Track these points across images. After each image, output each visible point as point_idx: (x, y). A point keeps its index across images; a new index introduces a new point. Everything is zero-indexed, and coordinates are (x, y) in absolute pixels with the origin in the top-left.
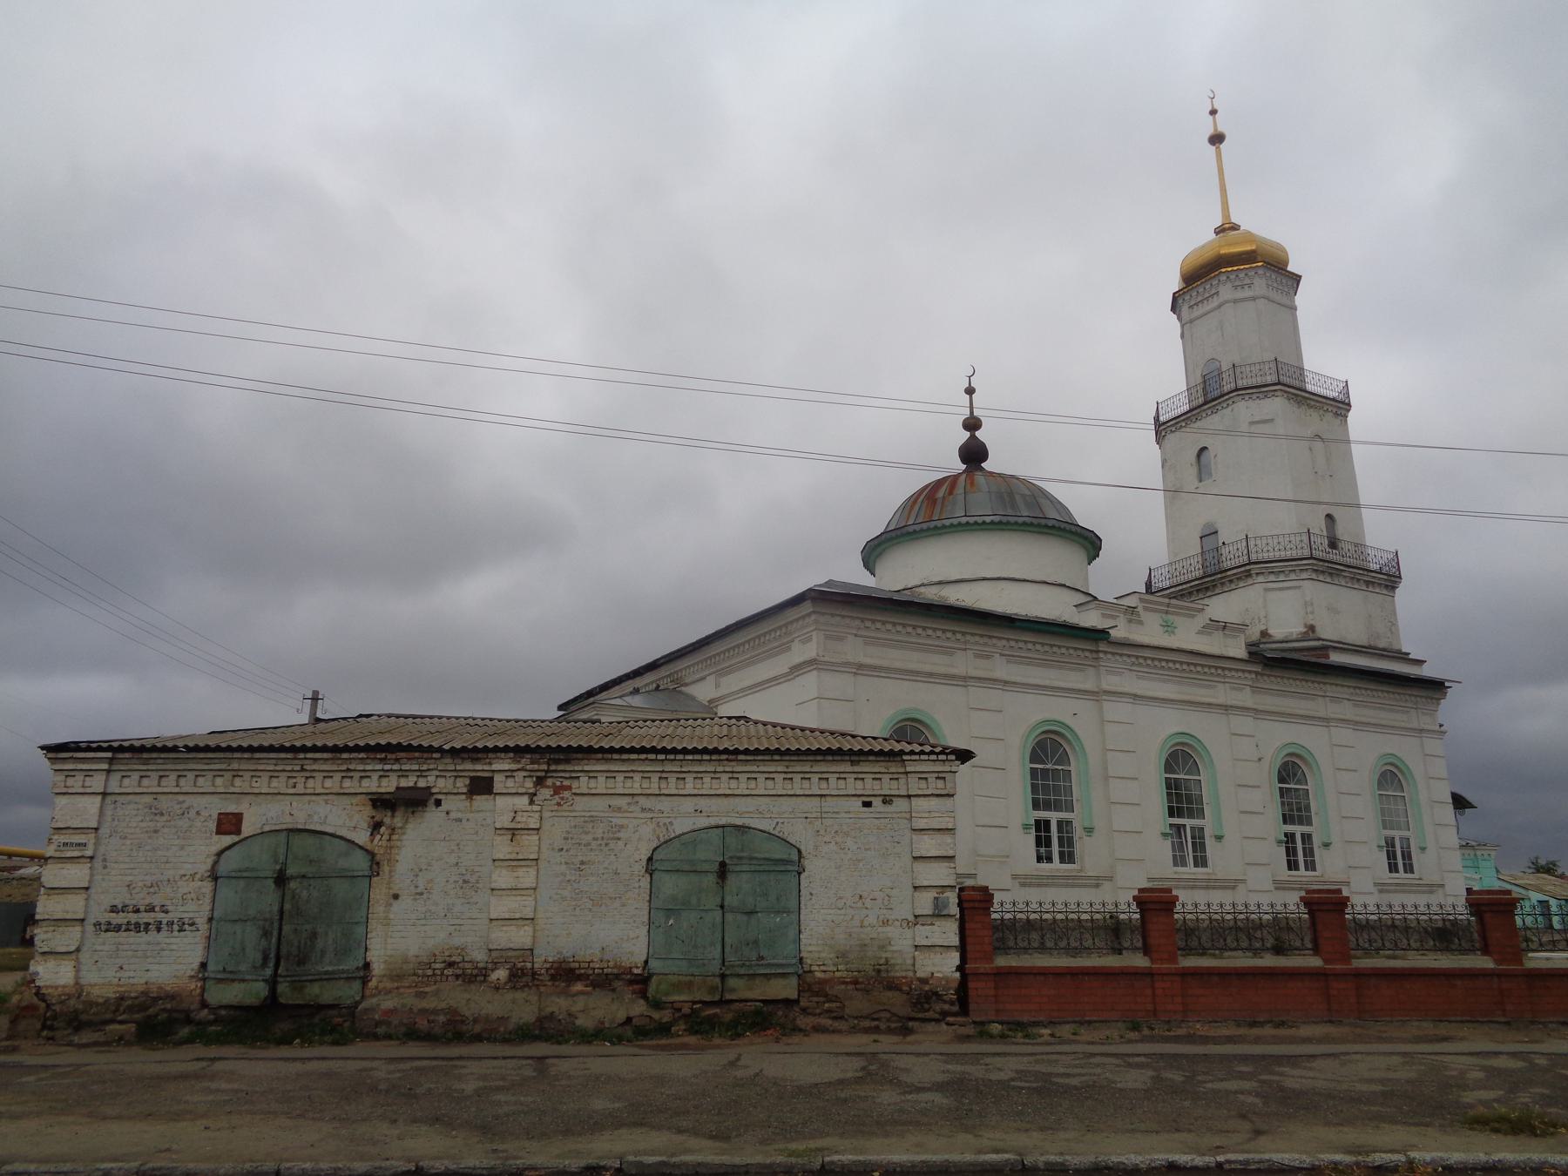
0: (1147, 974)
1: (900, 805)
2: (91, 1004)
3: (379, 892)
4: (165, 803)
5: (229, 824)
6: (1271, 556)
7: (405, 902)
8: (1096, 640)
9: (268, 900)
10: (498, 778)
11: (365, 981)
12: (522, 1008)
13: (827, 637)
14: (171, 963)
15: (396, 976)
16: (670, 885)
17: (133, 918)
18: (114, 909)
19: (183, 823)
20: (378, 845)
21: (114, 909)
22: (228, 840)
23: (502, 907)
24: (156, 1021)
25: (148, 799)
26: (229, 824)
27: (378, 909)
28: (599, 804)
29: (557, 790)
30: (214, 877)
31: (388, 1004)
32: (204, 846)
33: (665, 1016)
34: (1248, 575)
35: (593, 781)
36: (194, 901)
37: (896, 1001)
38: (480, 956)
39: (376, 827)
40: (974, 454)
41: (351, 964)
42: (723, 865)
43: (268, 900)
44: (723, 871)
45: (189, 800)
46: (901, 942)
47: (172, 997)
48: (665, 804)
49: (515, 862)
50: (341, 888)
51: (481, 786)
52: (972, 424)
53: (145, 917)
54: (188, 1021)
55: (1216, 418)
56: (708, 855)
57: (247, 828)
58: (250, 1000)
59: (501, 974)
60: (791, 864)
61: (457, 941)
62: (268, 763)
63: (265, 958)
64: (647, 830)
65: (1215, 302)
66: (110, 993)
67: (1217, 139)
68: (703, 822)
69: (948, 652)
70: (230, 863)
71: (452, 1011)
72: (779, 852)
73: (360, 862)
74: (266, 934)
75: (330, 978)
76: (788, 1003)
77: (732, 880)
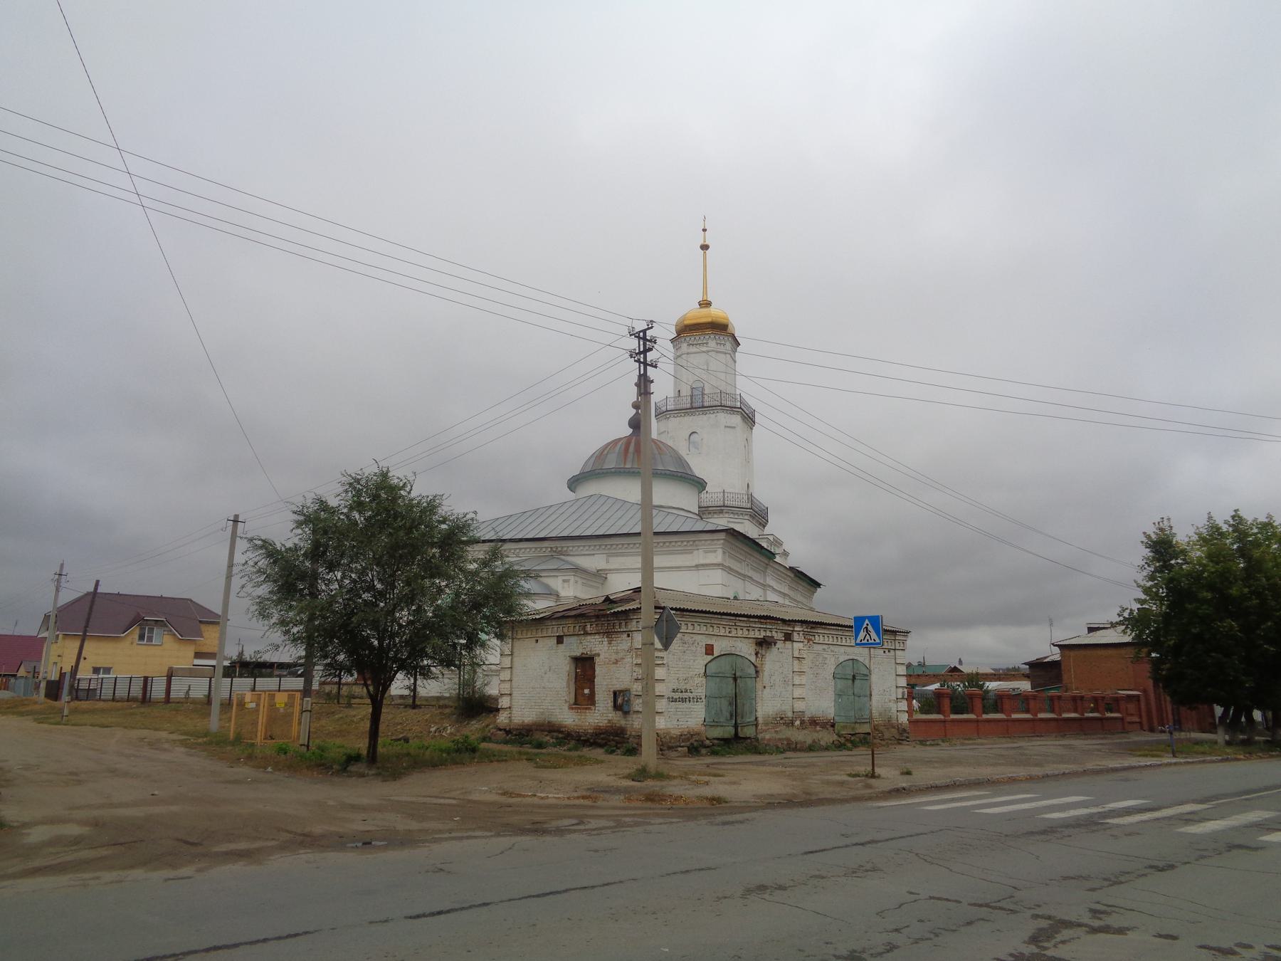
0: (945, 721)
2: (671, 738)
3: (759, 686)
5: (709, 650)
6: (734, 504)
7: (767, 690)
9: (729, 688)
11: (756, 726)
14: (692, 718)
15: (766, 724)
17: (681, 695)
18: (674, 691)
21: (674, 691)
22: (710, 658)
23: (798, 692)
24: (694, 746)
26: (709, 650)
28: (820, 647)
29: (809, 640)
31: (767, 737)
33: (842, 740)
34: (721, 512)
35: (821, 637)
36: (700, 687)
38: (790, 714)
39: (757, 654)
43: (729, 688)
44: (854, 677)
45: (696, 637)
46: (894, 707)
48: (836, 649)
50: (749, 682)
51: (788, 637)
53: (685, 695)
55: (705, 417)
56: (849, 672)
58: (726, 736)
59: (798, 723)
60: (866, 677)
66: (676, 732)
67: (705, 247)
68: (847, 658)
69: (740, 561)
70: (713, 668)
71: (788, 739)
73: (752, 671)
74: (730, 704)
77: (857, 682)
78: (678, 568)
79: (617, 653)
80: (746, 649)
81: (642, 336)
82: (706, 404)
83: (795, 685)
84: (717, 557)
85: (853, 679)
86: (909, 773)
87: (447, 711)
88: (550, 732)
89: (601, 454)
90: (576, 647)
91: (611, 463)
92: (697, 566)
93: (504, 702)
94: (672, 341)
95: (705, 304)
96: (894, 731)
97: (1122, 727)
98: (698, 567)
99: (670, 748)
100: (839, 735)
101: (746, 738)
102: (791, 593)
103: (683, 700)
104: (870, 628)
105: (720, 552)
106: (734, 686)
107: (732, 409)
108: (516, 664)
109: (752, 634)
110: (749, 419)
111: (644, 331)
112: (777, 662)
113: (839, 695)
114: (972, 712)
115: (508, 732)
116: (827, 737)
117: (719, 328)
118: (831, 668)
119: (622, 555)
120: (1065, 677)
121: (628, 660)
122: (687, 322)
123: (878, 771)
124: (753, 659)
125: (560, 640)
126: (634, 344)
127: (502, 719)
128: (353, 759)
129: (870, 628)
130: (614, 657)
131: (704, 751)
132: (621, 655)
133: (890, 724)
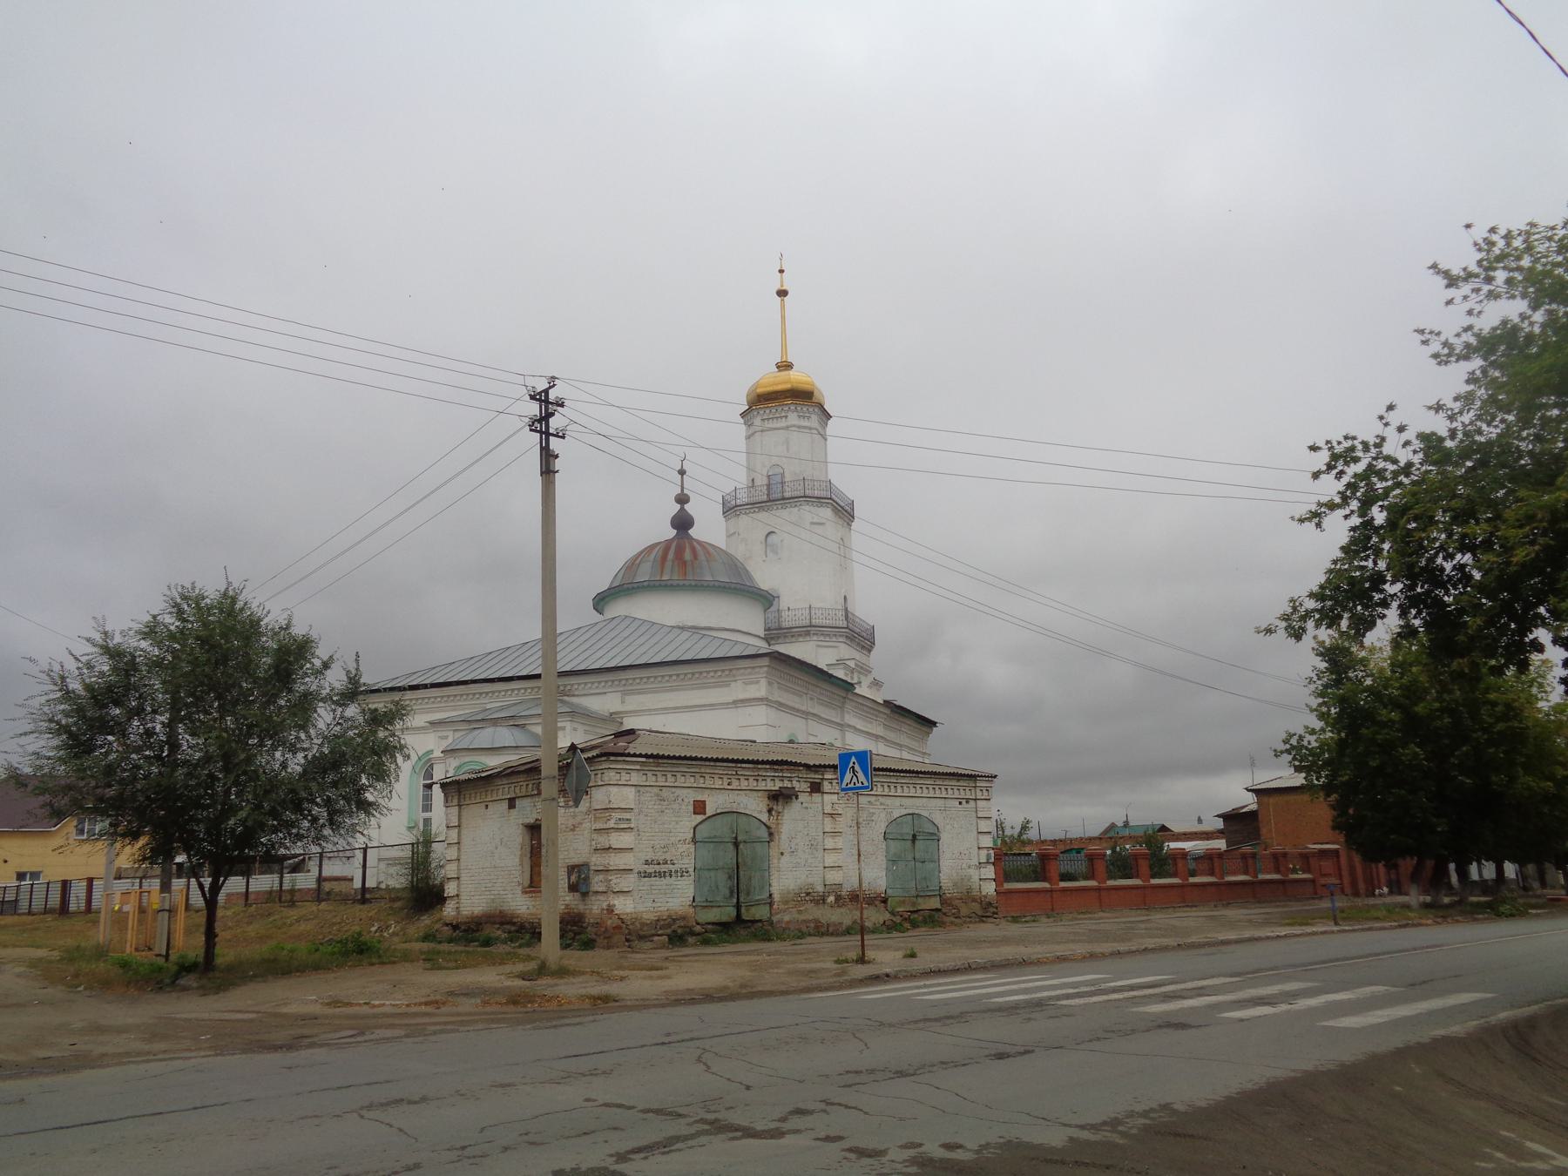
0: (1051, 891)
1: (972, 803)
2: (643, 924)
3: (774, 852)
4: (665, 793)
5: (699, 807)
6: (825, 622)
7: (785, 859)
8: (848, 690)
10: (826, 783)
11: (771, 904)
12: (845, 916)
13: (770, 684)
14: (678, 897)
18: (647, 862)
19: (676, 806)
20: (772, 822)
21: (647, 862)
22: (700, 818)
23: (830, 859)
24: (678, 934)
25: (656, 790)
26: (699, 807)
30: (694, 841)
31: (787, 918)
32: (687, 822)
33: (898, 919)
34: (808, 633)
37: (976, 907)
38: (820, 889)
39: (770, 811)
40: (682, 523)
42: (914, 836)
43: (728, 856)
45: (678, 791)
46: (975, 875)
47: (684, 918)
48: (888, 801)
49: (835, 833)
51: (816, 788)
52: (682, 499)
53: (663, 868)
54: (693, 934)
56: (907, 831)
57: (710, 811)
58: (725, 919)
59: (831, 899)
60: (934, 837)
61: (810, 880)
63: (732, 892)
64: (883, 815)
65: (782, 423)
66: (652, 917)
71: (817, 921)
72: (932, 830)
73: (763, 833)
75: (758, 903)
76: (937, 910)
78: (712, 706)
79: (574, 817)
80: (755, 805)
81: (542, 398)
82: (787, 495)
83: (823, 851)
84: (760, 689)
85: (915, 838)
86: (913, 955)
87: (398, 904)
88: (502, 924)
89: (632, 565)
90: (529, 811)
91: (644, 575)
92: (735, 702)
93: (450, 889)
94: (743, 415)
95: (785, 366)
96: (976, 907)
97: (1314, 890)
98: (737, 703)
99: (641, 938)
100: (893, 913)
101: (754, 922)
102: (891, 736)
103: (661, 875)
104: (857, 767)
105: (763, 682)
106: (737, 856)
107: (819, 500)
108: (466, 841)
109: (762, 785)
110: (845, 513)
111: (546, 391)
112: (798, 821)
113: (893, 861)
114: (1137, 877)
115: (455, 927)
116: (874, 916)
117: (802, 396)
119: (672, 689)
120: (1264, 831)
121: (587, 825)
122: (760, 390)
123: (870, 954)
124: (764, 817)
125: (512, 804)
126: (534, 409)
127: (449, 910)
128: (186, 968)
129: (857, 767)
130: (571, 822)
131: (691, 940)
132: (578, 819)
133: (969, 897)
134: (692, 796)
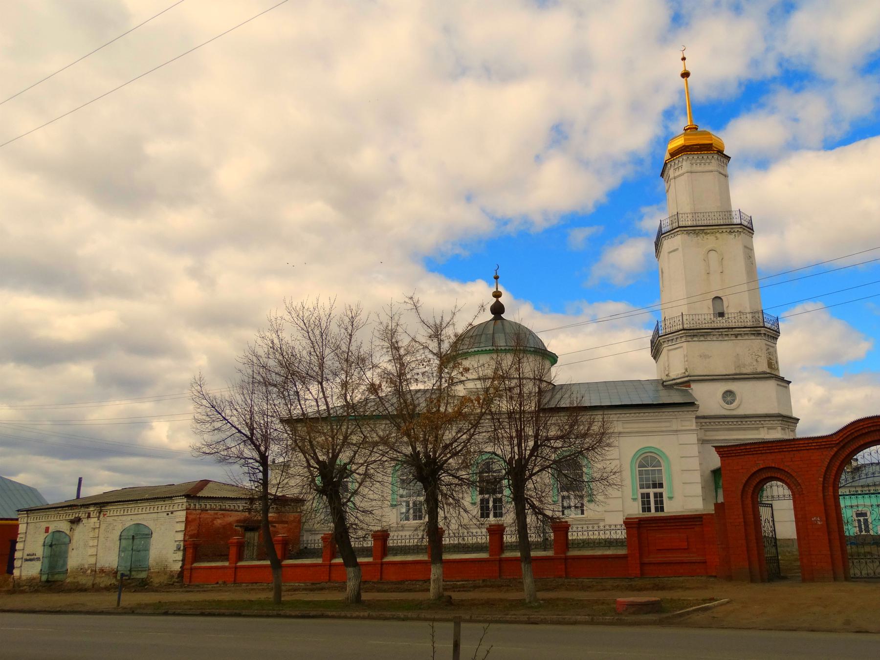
3: (70, 549)
15: (72, 572)
16: (124, 542)
27: (70, 553)
29: (104, 515)
41: (64, 569)
48: (124, 518)
50: (63, 547)
56: (131, 533)
59: (89, 571)
62: (52, 512)
85: (138, 538)
103: (31, 560)
113: (121, 550)
118: (117, 534)
134: (44, 525)
